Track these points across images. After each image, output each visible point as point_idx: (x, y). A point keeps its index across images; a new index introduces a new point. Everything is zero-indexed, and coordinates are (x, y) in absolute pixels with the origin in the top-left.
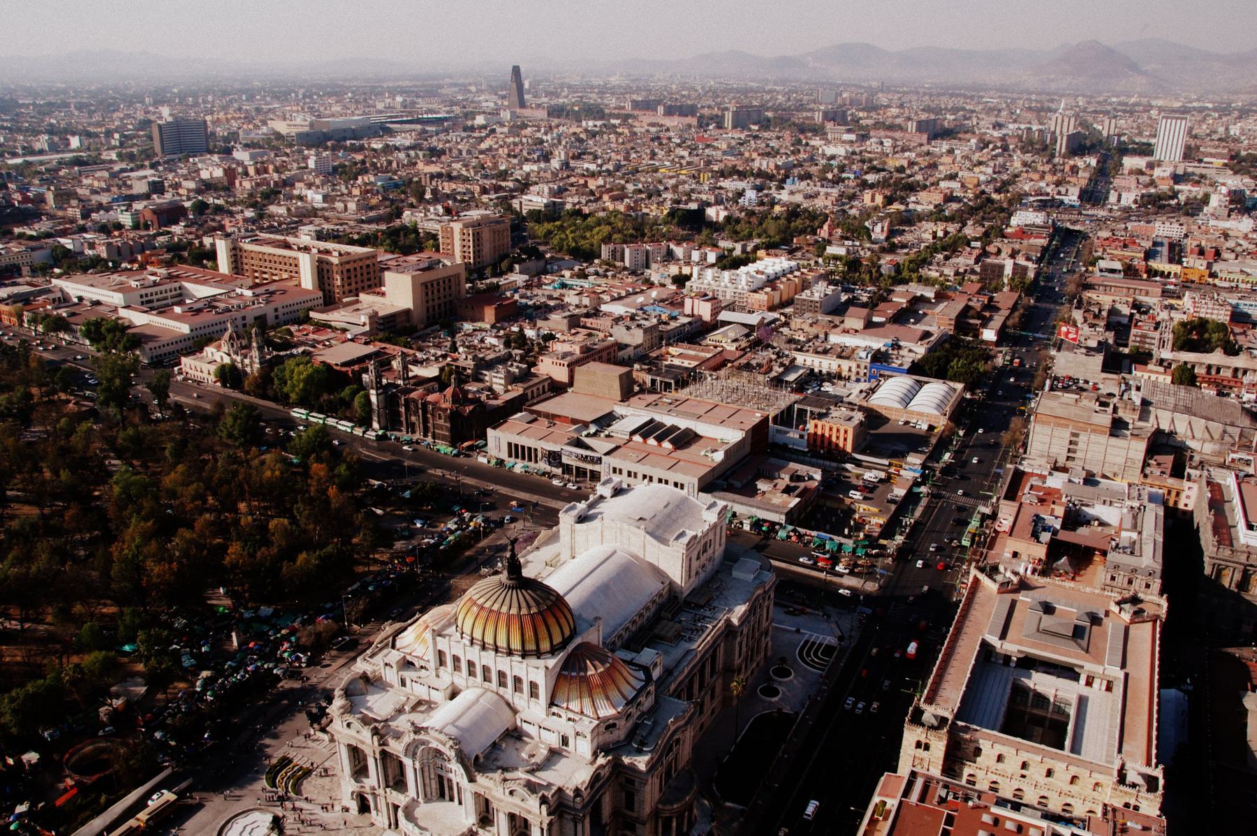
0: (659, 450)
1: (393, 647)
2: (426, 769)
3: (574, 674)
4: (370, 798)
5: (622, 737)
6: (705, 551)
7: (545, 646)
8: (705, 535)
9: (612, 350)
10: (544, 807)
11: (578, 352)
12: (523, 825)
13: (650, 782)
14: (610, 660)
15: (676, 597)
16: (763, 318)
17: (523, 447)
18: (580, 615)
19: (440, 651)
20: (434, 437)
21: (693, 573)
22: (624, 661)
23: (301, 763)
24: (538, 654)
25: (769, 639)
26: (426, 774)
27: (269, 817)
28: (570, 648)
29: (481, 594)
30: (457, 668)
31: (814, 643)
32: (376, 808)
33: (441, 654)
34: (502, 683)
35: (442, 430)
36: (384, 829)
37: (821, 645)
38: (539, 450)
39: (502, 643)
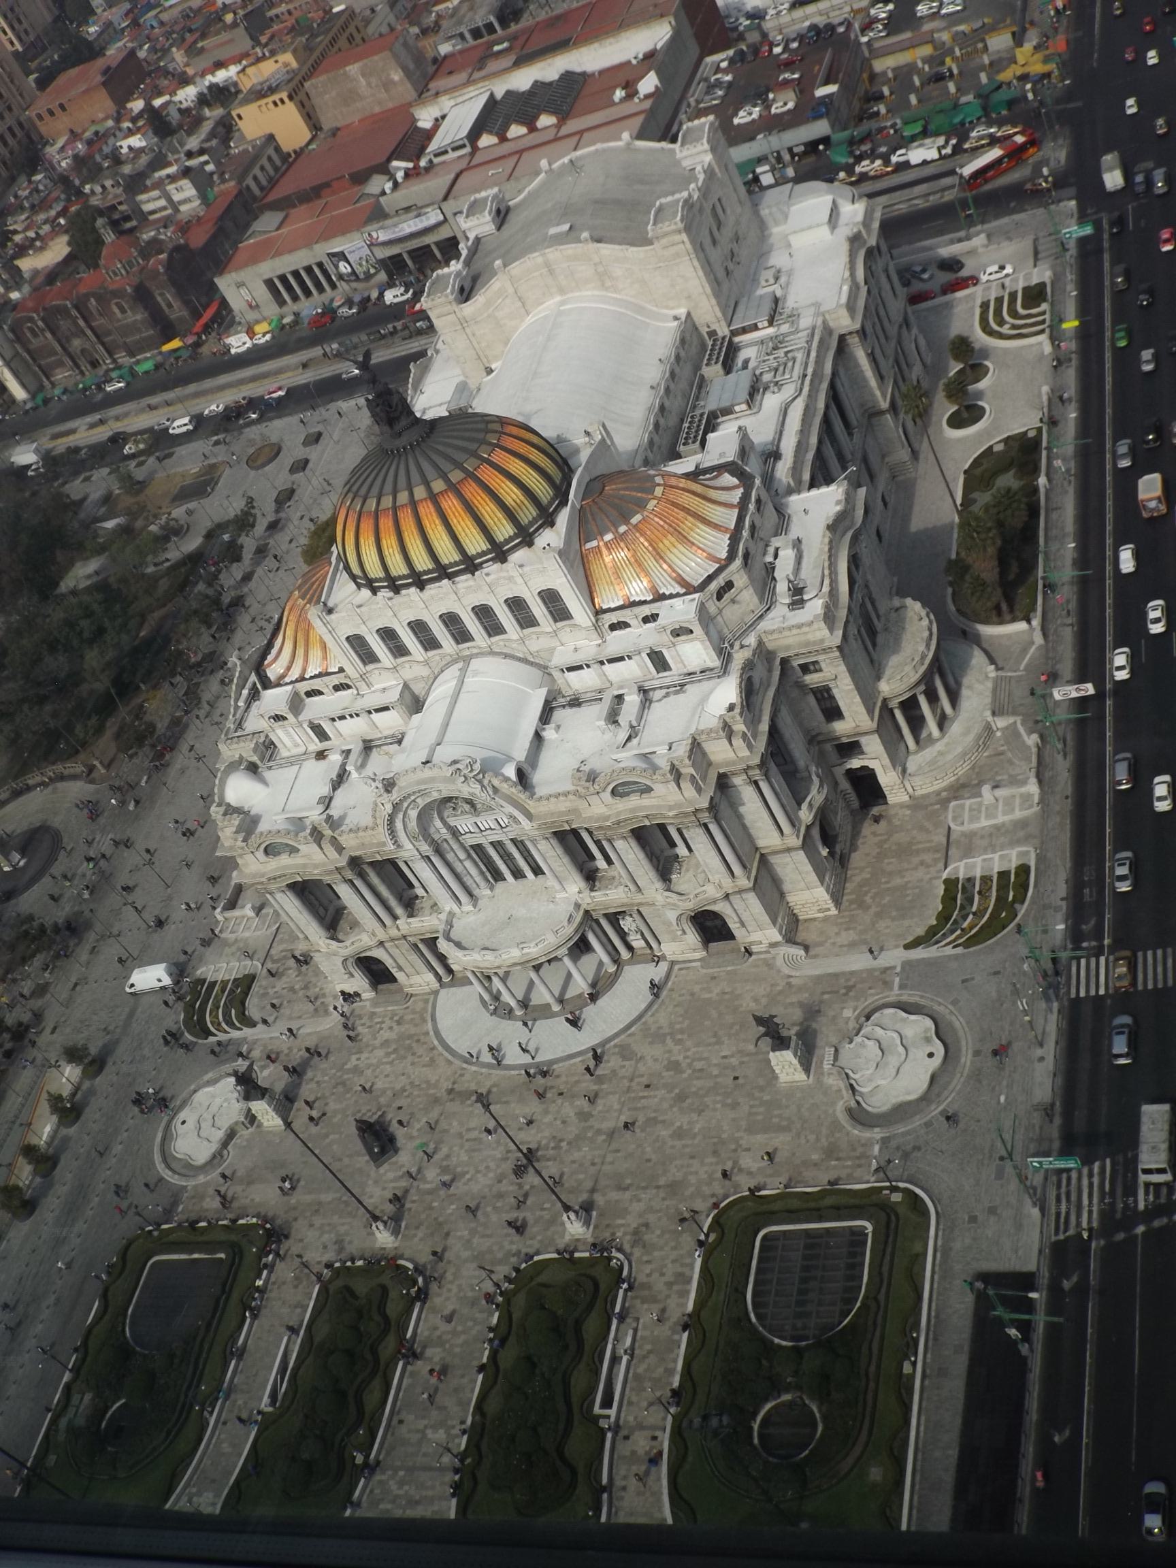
0: (535, 138)
1: (266, 684)
3: (609, 537)
7: (528, 513)
8: (705, 191)
9: (352, 29)
10: (686, 785)
11: (294, 65)
14: (659, 480)
17: (296, 274)
19: (348, 638)
20: (131, 354)
21: (721, 274)
22: (687, 476)
23: (227, 978)
24: (526, 537)
25: (915, 331)
27: (232, 1080)
29: (363, 491)
30: (399, 650)
31: (999, 300)
32: (400, 968)
33: (357, 643)
34: (493, 628)
37: (1013, 296)
38: (325, 260)
39: (448, 554)
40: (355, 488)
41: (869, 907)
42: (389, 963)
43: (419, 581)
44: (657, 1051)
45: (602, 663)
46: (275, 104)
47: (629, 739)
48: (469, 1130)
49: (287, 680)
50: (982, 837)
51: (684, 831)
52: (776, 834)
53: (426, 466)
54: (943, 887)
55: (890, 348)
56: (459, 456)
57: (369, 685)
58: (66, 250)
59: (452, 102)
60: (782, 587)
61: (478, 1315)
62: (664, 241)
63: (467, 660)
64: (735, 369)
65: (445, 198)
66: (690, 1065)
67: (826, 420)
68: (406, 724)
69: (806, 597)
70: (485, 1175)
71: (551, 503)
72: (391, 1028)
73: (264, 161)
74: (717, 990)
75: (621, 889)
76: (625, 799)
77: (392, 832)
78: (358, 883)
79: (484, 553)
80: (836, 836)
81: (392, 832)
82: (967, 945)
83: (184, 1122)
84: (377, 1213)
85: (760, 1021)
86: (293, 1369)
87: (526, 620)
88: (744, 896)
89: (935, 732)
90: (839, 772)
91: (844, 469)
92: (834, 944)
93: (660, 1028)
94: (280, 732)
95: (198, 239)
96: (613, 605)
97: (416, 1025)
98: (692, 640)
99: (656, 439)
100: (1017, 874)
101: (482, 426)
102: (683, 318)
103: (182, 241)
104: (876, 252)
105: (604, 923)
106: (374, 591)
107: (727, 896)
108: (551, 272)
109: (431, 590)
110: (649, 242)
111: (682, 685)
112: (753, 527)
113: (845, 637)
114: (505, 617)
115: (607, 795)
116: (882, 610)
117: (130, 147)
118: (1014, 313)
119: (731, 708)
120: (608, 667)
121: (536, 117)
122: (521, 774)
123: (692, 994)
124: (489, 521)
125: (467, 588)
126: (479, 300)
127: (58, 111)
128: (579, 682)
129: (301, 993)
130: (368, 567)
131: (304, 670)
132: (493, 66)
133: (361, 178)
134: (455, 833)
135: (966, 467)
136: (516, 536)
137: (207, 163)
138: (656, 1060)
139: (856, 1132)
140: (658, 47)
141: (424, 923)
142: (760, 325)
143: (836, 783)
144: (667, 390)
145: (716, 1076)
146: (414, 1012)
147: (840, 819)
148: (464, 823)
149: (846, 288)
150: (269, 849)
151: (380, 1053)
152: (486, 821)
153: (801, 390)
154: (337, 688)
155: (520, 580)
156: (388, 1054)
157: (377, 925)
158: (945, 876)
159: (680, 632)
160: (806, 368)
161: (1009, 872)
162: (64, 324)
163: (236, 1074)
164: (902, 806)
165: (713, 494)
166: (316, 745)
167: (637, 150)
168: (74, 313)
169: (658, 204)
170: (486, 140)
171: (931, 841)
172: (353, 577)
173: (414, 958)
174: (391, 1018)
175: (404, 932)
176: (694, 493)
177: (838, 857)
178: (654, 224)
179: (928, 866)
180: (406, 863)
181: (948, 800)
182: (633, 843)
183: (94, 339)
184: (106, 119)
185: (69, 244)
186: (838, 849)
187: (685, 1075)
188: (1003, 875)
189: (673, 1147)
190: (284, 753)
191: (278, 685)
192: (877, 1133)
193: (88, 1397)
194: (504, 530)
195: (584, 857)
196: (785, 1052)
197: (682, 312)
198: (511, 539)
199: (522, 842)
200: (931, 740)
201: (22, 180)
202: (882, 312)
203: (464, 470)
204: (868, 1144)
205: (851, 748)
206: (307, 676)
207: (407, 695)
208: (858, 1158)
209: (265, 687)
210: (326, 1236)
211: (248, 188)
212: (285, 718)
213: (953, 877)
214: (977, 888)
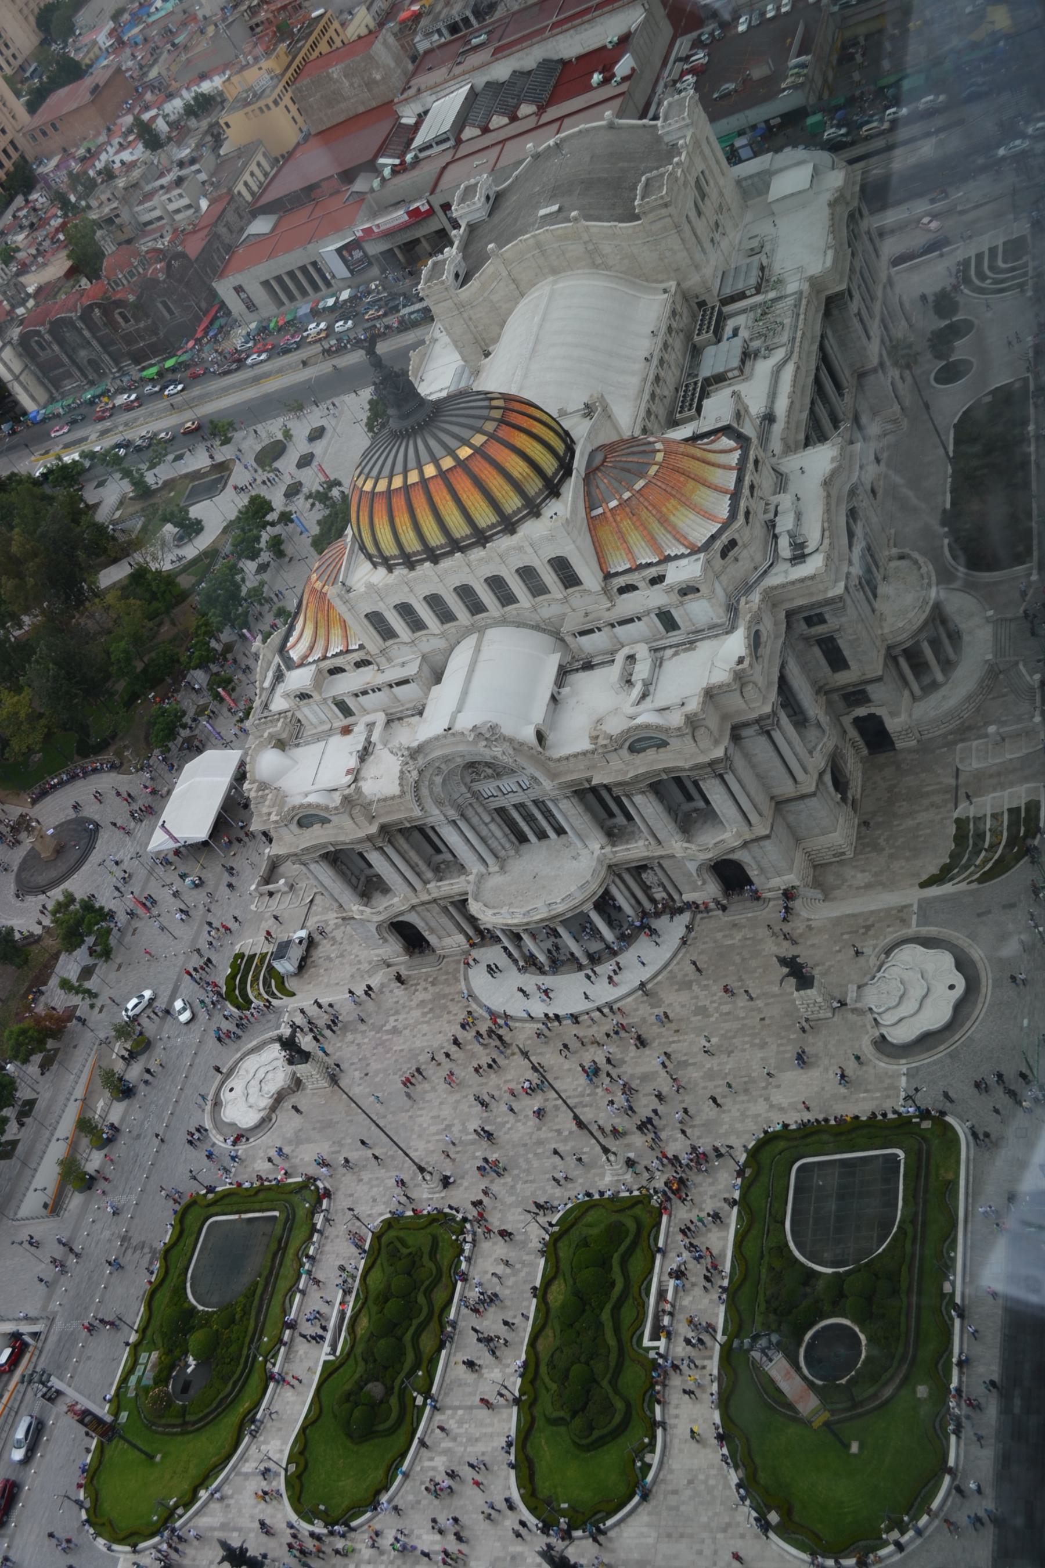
1: (290, 665)
2: (470, 813)
4: (412, 918)
5: (758, 557)
6: (703, 196)
7: (534, 486)
9: (331, 32)
12: (679, 797)
13: (849, 601)
14: (659, 446)
15: (702, 304)
17: (291, 274)
18: (563, 413)
19: (366, 616)
20: (137, 361)
22: (687, 440)
24: (534, 510)
26: (475, 820)
29: (374, 473)
30: (417, 624)
32: (432, 931)
33: (376, 619)
34: (507, 598)
35: (143, 338)
39: (459, 528)
40: (366, 471)
41: (883, 849)
42: (420, 925)
43: (434, 557)
44: (684, 997)
45: (613, 626)
46: (260, 109)
47: (644, 696)
48: (506, 1082)
49: (310, 659)
50: (991, 776)
51: (701, 783)
52: (790, 782)
53: (432, 443)
54: (954, 826)
56: (465, 433)
57: (389, 660)
58: (68, 264)
59: (434, 97)
60: (784, 542)
61: (525, 1258)
62: (651, 216)
63: (481, 630)
64: (725, 337)
65: (432, 192)
66: (717, 1009)
67: (817, 382)
68: (427, 695)
69: (807, 551)
70: (524, 1124)
71: (555, 474)
72: (426, 989)
73: (253, 167)
74: (739, 936)
75: (641, 843)
76: (642, 755)
78: (389, 850)
79: (493, 526)
80: (847, 783)
81: (419, 799)
82: (981, 880)
83: (231, 1090)
84: (423, 1164)
85: (783, 961)
86: (351, 1317)
87: (538, 589)
88: (762, 843)
89: (940, 677)
90: (847, 721)
91: (836, 427)
92: (850, 886)
93: (686, 975)
94: (306, 710)
95: (193, 247)
96: (620, 569)
97: (449, 985)
98: (698, 599)
99: (654, 408)
100: (1027, 810)
101: (486, 403)
102: (673, 290)
103: (180, 248)
104: (857, 215)
105: (627, 877)
106: (390, 569)
107: (745, 844)
108: (543, 253)
109: (445, 564)
110: (637, 217)
111: (692, 642)
112: (752, 487)
113: (846, 588)
114: (517, 586)
115: (624, 752)
117: (122, 162)
119: (741, 661)
120: (618, 630)
121: (517, 107)
122: (540, 736)
123: (715, 941)
124: (498, 494)
125: (480, 560)
126: (474, 284)
127: (50, 130)
128: (589, 644)
129: (337, 961)
130: (383, 546)
131: (327, 650)
132: (474, 60)
134: (477, 795)
135: (956, 421)
136: (524, 507)
137: (199, 171)
138: (683, 1006)
139: (882, 1064)
140: (633, 28)
141: (451, 886)
142: (748, 293)
143: (845, 732)
144: (662, 361)
145: (743, 1018)
146: (447, 973)
147: (853, 768)
149: (830, 254)
150: (304, 821)
151: (416, 1014)
152: (508, 784)
153: (792, 352)
154: (359, 665)
155: (530, 550)
156: (424, 1014)
157: (408, 890)
158: (956, 815)
159: (688, 590)
160: (796, 332)
161: (1019, 809)
162: (69, 335)
163: (280, 1039)
164: (910, 751)
165: (712, 457)
166: (341, 721)
167: (620, 128)
168: (80, 324)
169: (643, 179)
170: (468, 133)
171: (939, 783)
172: (369, 557)
173: (445, 920)
174: (426, 980)
175: (435, 895)
176: (694, 457)
177: (850, 802)
178: (642, 199)
179: (938, 807)
180: (433, 828)
181: (955, 743)
182: (652, 797)
183: (99, 349)
184: (98, 134)
185: (69, 257)
186: (850, 796)
187: (713, 1019)
188: (1014, 812)
189: (705, 1088)
190: (309, 732)
191: (301, 665)
192: (903, 1066)
193: (155, 1355)
194: (512, 502)
195: (603, 814)
196: (809, 991)
197: (672, 285)
198: (519, 510)
199: (543, 802)
200: (934, 686)
201: (19, 201)
202: (867, 274)
203: (471, 446)
204: (897, 1075)
205: (856, 696)
206: (329, 655)
207: (426, 669)
208: (886, 1089)
209: (289, 668)
210: (375, 1189)
211: (239, 193)
212: (309, 697)
213: (963, 817)
214: (988, 826)
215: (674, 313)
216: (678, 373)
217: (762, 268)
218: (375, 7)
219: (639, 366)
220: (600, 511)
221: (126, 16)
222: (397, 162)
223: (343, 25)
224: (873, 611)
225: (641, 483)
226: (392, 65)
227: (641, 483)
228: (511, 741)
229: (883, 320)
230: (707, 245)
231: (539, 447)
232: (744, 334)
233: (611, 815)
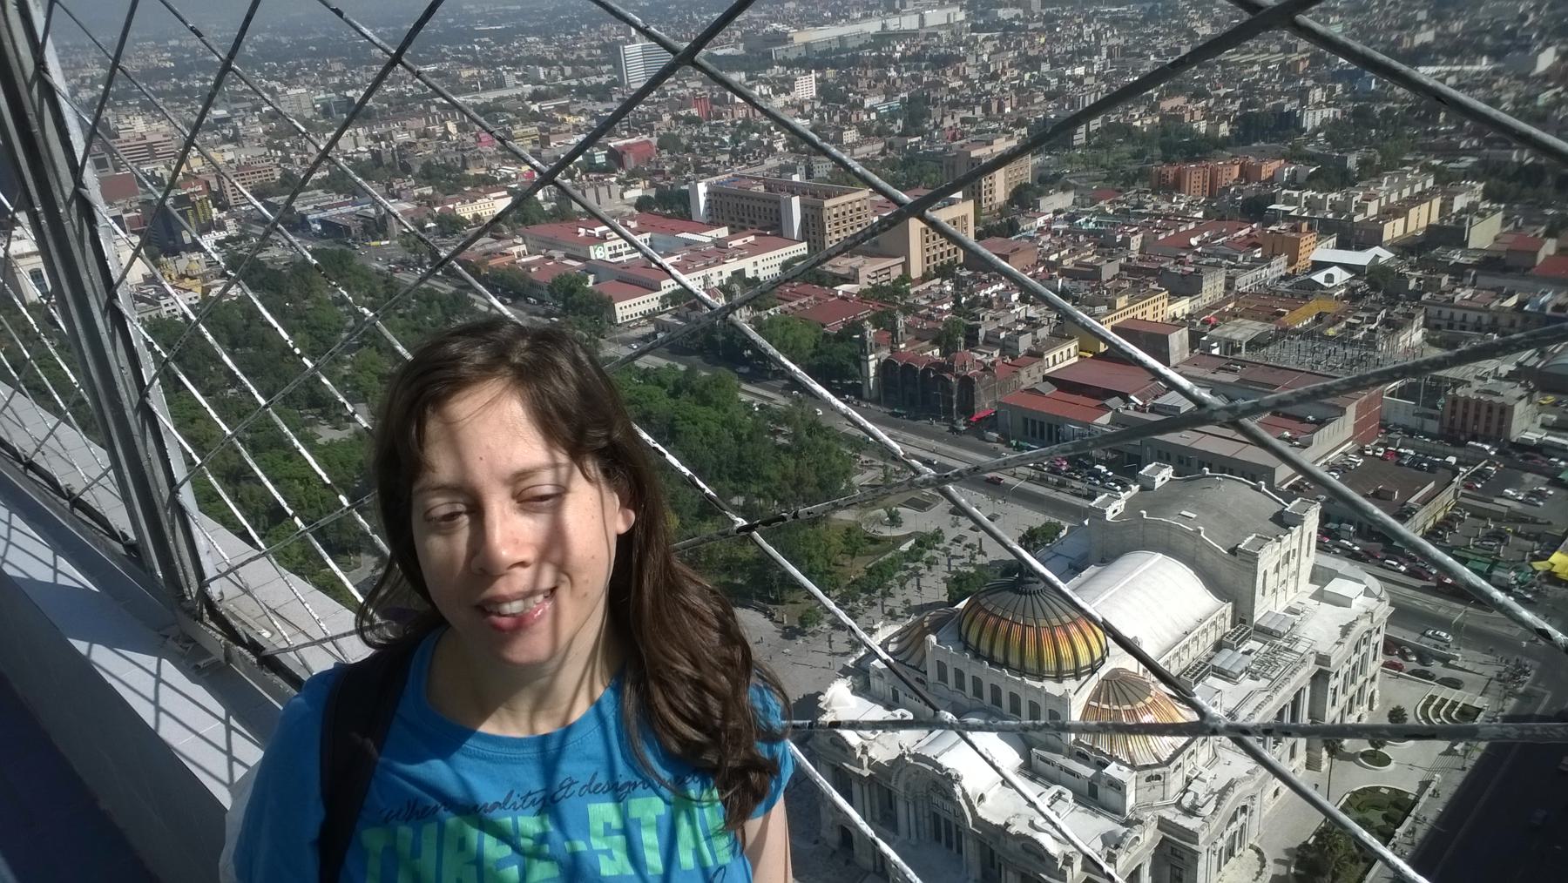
2: (920, 804)
3: (1106, 706)
9: (1160, 303)
16: (1377, 257)
17: (1042, 423)
24: (1059, 678)
25: (1375, 685)
26: (920, 810)
28: (1103, 672)
30: (960, 684)
31: (1444, 701)
36: (868, 873)
55: (1352, 689)
73: (1065, 350)
77: (897, 777)
104: (1374, 631)
112: (1193, 753)
116: (1246, 845)
118: (1447, 715)
120: (1063, 773)
133: (1111, 394)
148: (937, 799)
152: (948, 806)
172: (960, 634)
182: (1019, 879)
201: (937, 281)
215: (1223, 616)
216: (1201, 651)
217: (1293, 625)
218: (1195, 302)
219: (1179, 633)
220: (1096, 704)
221: (1062, 216)
222: (1141, 403)
223: (1170, 302)
224: (1219, 870)
225: (1129, 707)
226: (1177, 348)
227: (1129, 707)
228: (963, 790)
229: (1351, 700)
230: (1268, 591)
231: (1085, 648)
232: (1253, 656)
233: (993, 866)
